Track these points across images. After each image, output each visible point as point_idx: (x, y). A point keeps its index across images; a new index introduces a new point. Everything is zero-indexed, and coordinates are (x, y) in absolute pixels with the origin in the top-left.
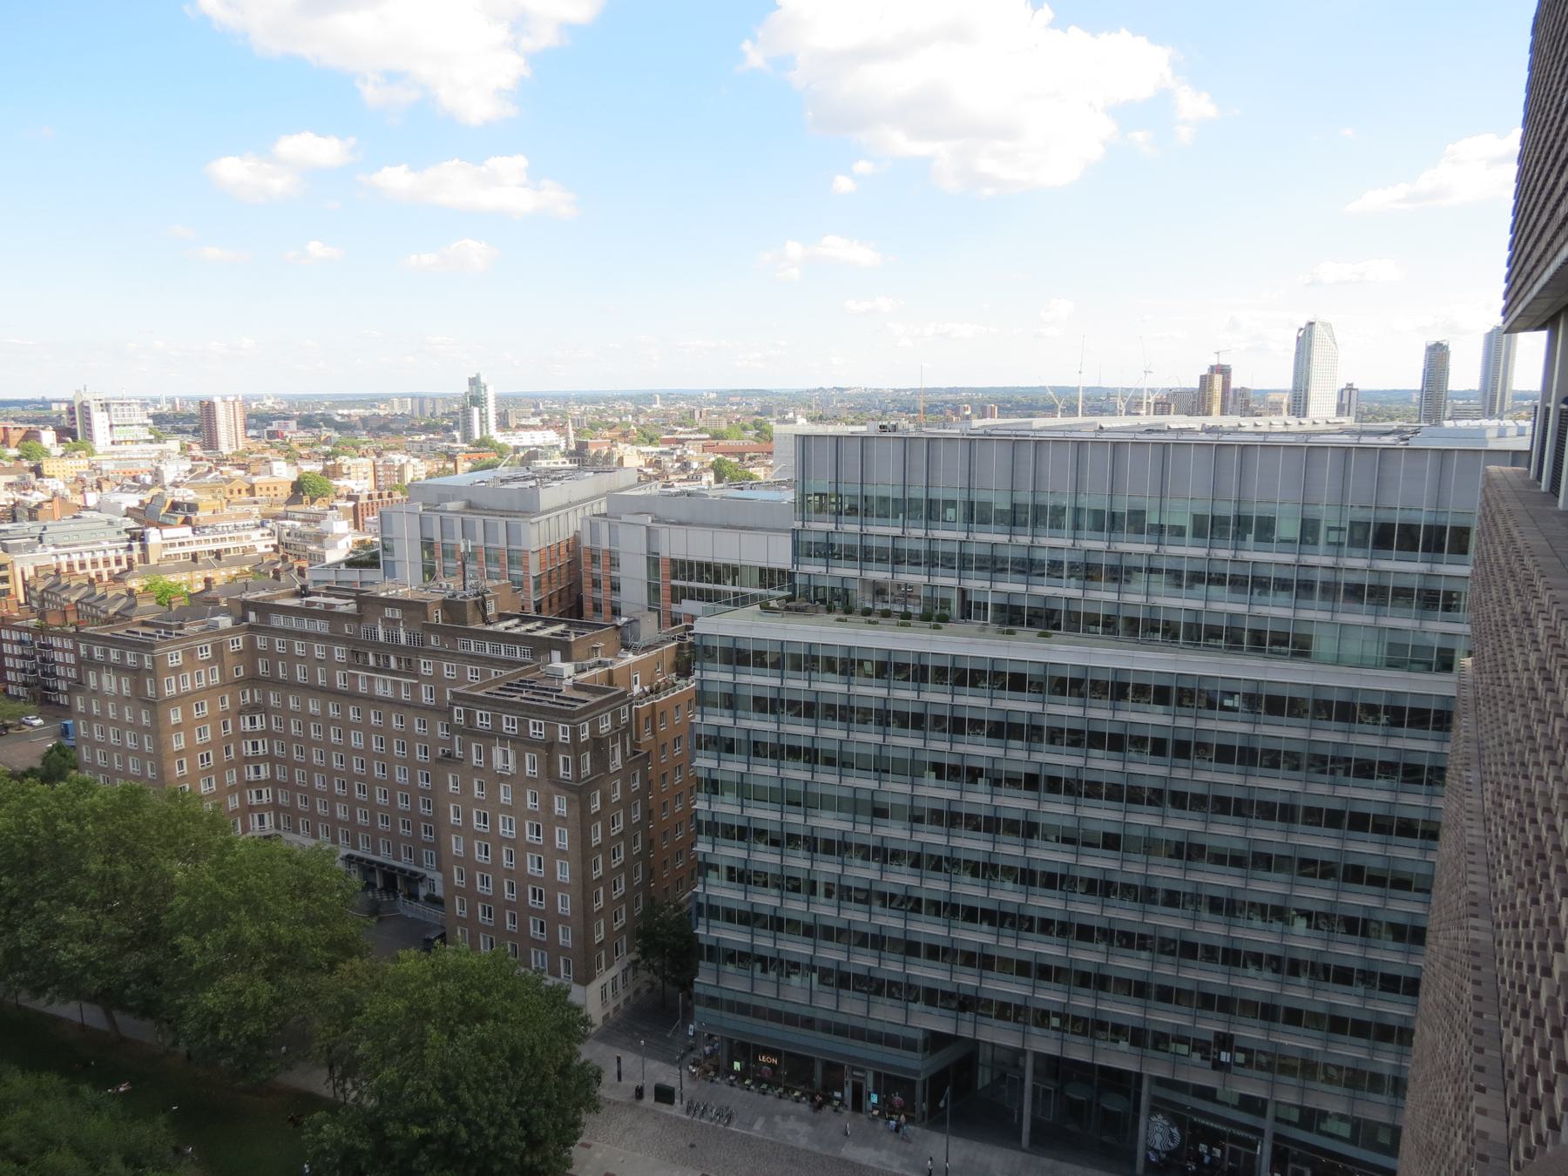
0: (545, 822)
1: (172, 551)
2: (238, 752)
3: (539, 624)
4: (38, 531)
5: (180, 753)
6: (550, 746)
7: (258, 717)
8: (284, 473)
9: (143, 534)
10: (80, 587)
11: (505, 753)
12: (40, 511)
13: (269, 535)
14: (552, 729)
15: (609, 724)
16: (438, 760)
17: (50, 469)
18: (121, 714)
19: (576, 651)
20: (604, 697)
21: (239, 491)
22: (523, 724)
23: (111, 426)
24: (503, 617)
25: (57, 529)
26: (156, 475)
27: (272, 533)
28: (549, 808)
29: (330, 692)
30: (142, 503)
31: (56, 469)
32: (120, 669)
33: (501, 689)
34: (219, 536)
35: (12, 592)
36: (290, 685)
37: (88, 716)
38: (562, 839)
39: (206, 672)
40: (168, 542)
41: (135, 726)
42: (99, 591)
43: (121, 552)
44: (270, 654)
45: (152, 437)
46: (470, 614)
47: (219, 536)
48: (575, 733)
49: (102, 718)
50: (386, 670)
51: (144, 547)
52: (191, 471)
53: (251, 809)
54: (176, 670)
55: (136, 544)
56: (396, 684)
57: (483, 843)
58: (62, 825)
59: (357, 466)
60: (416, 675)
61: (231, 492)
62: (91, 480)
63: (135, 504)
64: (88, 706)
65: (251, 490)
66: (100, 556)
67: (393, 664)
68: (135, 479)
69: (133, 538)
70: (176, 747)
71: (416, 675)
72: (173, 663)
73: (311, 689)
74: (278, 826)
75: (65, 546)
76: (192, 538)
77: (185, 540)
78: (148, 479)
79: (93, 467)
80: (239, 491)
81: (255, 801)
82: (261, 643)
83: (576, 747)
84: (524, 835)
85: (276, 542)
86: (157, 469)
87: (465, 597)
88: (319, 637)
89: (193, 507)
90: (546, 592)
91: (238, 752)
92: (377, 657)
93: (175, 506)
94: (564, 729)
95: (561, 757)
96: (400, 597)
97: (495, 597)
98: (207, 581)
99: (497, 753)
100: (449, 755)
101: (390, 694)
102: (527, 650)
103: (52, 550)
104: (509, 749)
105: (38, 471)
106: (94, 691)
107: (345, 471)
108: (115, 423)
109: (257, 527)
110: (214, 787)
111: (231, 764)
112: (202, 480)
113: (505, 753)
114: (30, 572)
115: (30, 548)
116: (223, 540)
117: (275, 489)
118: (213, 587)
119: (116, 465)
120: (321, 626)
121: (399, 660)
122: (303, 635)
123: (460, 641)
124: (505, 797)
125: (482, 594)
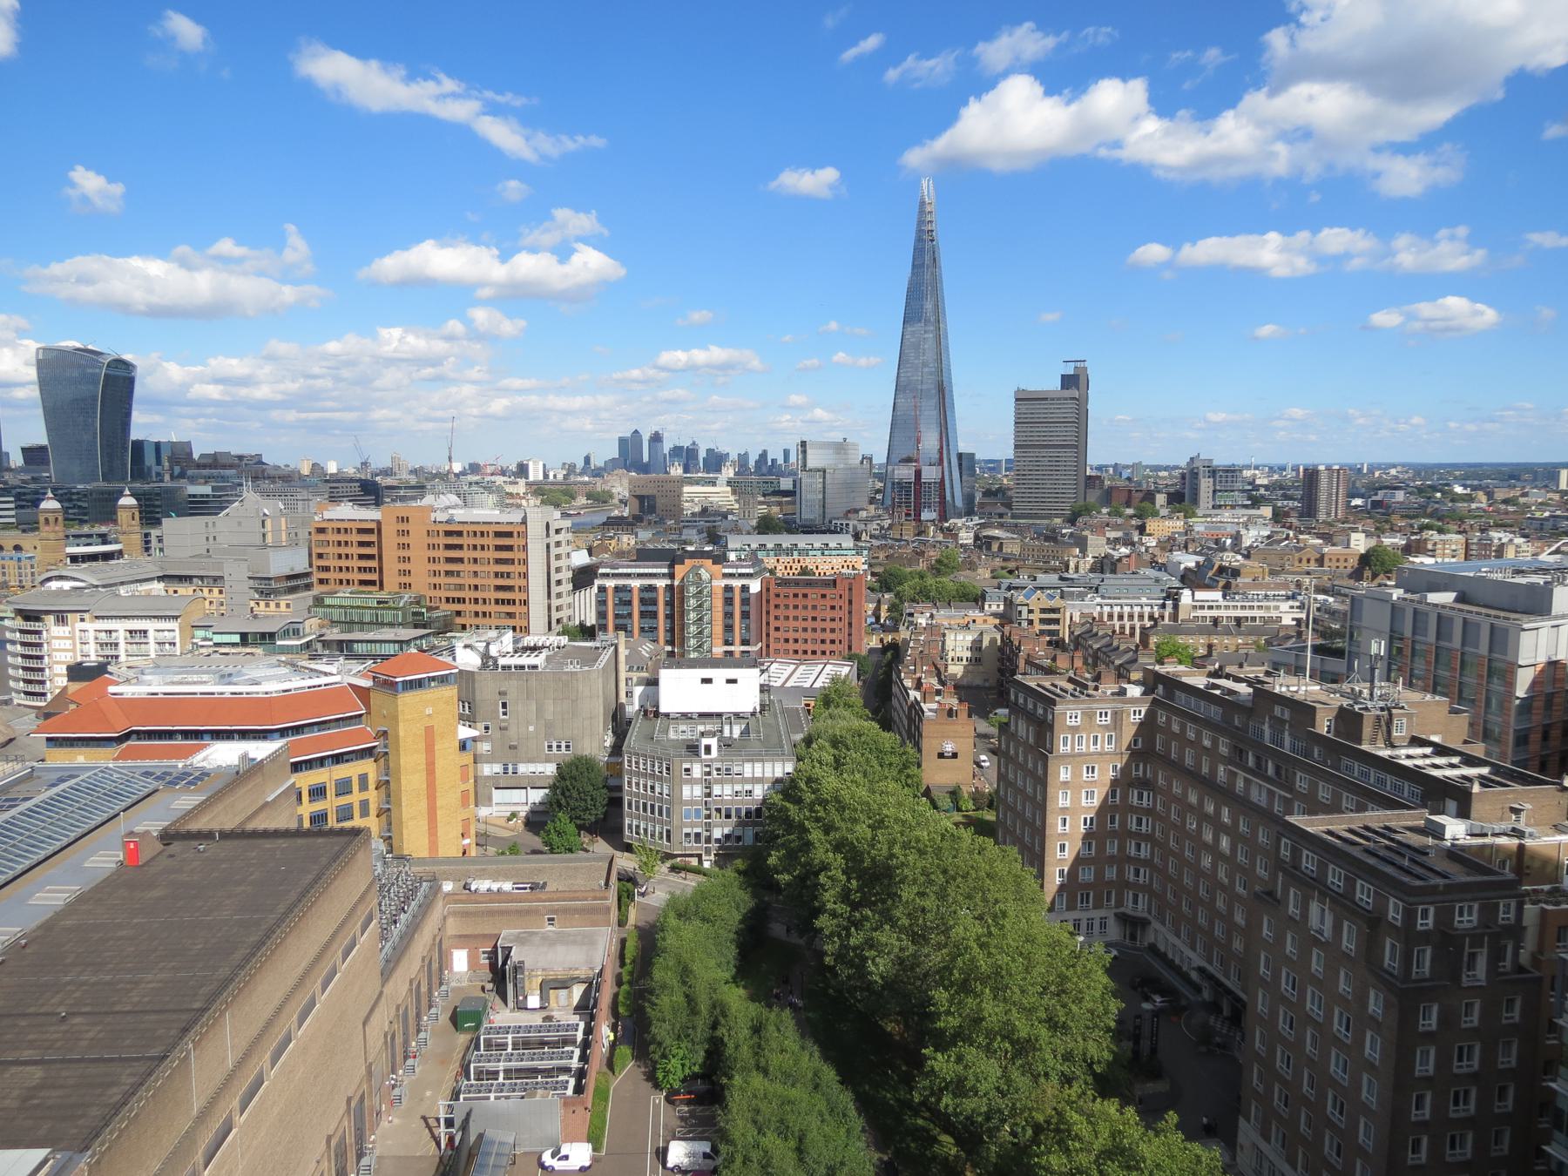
0: (1360, 1021)
2: (1123, 823)
3: (1455, 760)
4: (1097, 582)
5: (1064, 810)
6: (1373, 923)
7: (1145, 794)
8: (1360, 543)
9: (1177, 594)
10: (1107, 635)
11: (1323, 910)
12: (1119, 565)
13: (1298, 607)
14: (1381, 901)
15: (1475, 917)
16: (1256, 895)
18: (1026, 761)
19: (1476, 807)
20: (1486, 878)
21: (1308, 561)
22: (1350, 883)
23: (1214, 491)
24: (1416, 741)
25: (1112, 582)
27: (1301, 607)
28: (1363, 1001)
29: (1208, 785)
30: (1197, 563)
33: (1351, 831)
34: (1247, 604)
36: (1177, 768)
38: (1372, 1048)
39: (1103, 737)
41: (1032, 774)
42: (1115, 643)
43: (1156, 608)
44: (1167, 730)
46: (1367, 730)
47: (1247, 604)
48: (1409, 915)
50: (1259, 771)
51: (1176, 607)
52: (1269, 537)
53: (1128, 885)
54: (1074, 730)
55: (1169, 603)
56: (1271, 793)
57: (1290, 1013)
58: (896, 850)
59: (1444, 542)
60: (1291, 789)
61: (1300, 561)
62: (1181, 539)
63: (1192, 565)
65: (1320, 561)
66: (1137, 609)
67: (1271, 771)
68: (1217, 542)
69: (1167, 597)
70: (1061, 803)
71: (1291, 789)
73: (1194, 777)
74: (1149, 912)
76: (1222, 603)
77: (1214, 604)
78: (1229, 541)
79: (1188, 530)
80: (1308, 561)
81: (1132, 878)
82: (1162, 719)
83: (1409, 936)
84: (1332, 1024)
85: (1303, 616)
86: (1238, 532)
87: (1366, 709)
88: (1207, 723)
89: (1236, 573)
90: (1538, 718)
91: (1123, 823)
92: (1258, 759)
93: (1222, 570)
94: (1508, 906)
95: (1388, 942)
96: (1300, 697)
97: (1410, 716)
98: (1210, 646)
99: (1314, 907)
100: (1271, 894)
101: (1264, 804)
102: (1418, 790)
103: (1099, 600)
104: (1326, 908)
105: (1142, 529)
107: (1430, 547)
109: (1288, 598)
110: (1093, 852)
111: (1113, 834)
112: (1275, 547)
113: (1323, 910)
114: (1077, 619)
115: (1082, 596)
116: (1252, 608)
117: (1346, 560)
118: (1214, 653)
119: (1206, 528)
120: (1215, 712)
121: (1278, 770)
122: (1194, 719)
123: (1346, 761)
124: (1316, 966)
125: (1389, 709)
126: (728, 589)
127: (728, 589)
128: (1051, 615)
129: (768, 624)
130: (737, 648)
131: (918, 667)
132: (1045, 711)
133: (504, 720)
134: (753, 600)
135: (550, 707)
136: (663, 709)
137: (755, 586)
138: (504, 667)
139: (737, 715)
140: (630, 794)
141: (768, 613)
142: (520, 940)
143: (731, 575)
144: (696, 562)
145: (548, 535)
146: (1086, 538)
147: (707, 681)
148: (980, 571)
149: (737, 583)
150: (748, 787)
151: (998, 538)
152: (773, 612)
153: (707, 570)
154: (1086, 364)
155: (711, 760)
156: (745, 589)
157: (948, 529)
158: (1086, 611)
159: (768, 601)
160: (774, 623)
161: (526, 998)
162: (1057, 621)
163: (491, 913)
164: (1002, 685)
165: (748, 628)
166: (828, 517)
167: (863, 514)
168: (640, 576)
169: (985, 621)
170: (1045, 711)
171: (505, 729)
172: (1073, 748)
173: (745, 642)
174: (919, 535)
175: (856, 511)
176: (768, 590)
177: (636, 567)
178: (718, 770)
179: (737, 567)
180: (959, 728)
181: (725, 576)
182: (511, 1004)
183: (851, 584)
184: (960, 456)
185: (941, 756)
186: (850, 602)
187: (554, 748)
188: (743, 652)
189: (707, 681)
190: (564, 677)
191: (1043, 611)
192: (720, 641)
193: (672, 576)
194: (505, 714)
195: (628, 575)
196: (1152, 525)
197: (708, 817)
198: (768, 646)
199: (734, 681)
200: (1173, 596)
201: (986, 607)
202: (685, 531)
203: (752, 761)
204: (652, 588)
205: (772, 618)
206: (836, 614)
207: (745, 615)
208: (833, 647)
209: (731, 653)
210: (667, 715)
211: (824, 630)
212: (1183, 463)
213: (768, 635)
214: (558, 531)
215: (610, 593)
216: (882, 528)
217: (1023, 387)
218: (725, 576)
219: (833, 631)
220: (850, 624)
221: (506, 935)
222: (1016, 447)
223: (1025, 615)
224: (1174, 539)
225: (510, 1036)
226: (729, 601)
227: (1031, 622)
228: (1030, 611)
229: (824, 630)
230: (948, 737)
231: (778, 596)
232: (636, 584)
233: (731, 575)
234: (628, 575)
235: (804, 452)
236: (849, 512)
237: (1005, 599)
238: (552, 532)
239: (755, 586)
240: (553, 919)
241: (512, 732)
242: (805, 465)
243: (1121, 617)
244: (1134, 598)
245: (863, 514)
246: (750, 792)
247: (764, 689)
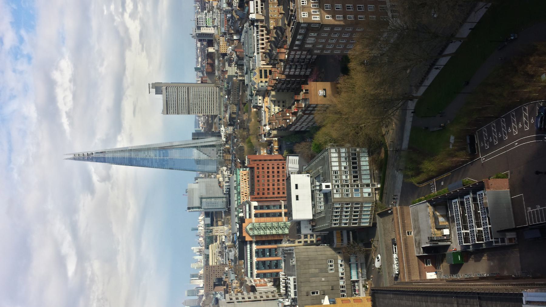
1: (260, 10)
9: (251, 21)
17: (223, 50)
18: (324, 38)
23: (207, 27)
26: (227, 12)
31: (223, 49)
32: (305, 36)
35: (270, 69)
37: (322, 49)
40: (255, 11)
41: (330, 33)
42: (273, 39)
45: (211, 12)
49: (324, 45)
51: (257, 21)
64: (318, 49)
72: (306, 16)
75: (254, 49)
103: (255, 54)
105: (224, 55)
106: (313, 46)
108: (205, 25)
114: (263, 62)
115: (254, 61)
126: (256, 216)
127: (256, 216)
128: (264, 74)
129: (271, 198)
130: (283, 211)
131: (287, 118)
132: (302, 28)
133: (320, 293)
134: (261, 204)
135: (313, 271)
136: (311, 217)
137: (255, 204)
138: (295, 295)
139: (312, 183)
140: (350, 223)
141: (266, 198)
142: (419, 244)
143: (250, 214)
144: (244, 231)
145: (233, 302)
146: (229, 76)
147: (297, 197)
148: (245, 119)
149: (253, 212)
150: (343, 168)
151: (230, 115)
152: (266, 195)
153: (247, 226)
154: (151, 83)
155: (332, 185)
156: (256, 208)
157: (226, 139)
158: (260, 59)
159: (261, 198)
160: (271, 195)
161: (445, 235)
162: (266, 71)
163: (408, 261)
164: (294, 89)
165: (274, 206)
166: (222, 195)
167: (221, 179)
168: (251, 257)
169: (267, 102)
170: (302, 28)
171: (324, 292)
172: (318, 15)
173: (280, 208)
174: (229, 152)
175: (220, 183)
176: (256, 198)
177: (247, 260)
178: (336, 181)
179: (246, 212)
180: (313, 88)
181: (250, 217)
182: (449, 243)
183: (252, 161)
184: (193, 139)
185: (325, 96)
186: (260, 160)
187: (332, 268)
188: (284, 208)
189: (297, 197)
190: (299, 264)
191: (261, 77)
192: (280, 218)
193: (251, 243)
194: (317, 293)
195: (251, 263)
196: (222, 51)
197: (358, 186)
198: (281, 197)
199: (297, 186)
200: (253, 21)
201: (260, 105)
202: (230, 258)
203: (331, 166)
204: (258, 263)
205: (269, 196)
206: (266, 166)
207: (268, 207)
208: (281, 167)
209: (285, 214)
210: (314, 216)
211: (273, 172)
212: (194, 40)
213: (277, 198)
214: (231, 299)
215: (260, 271)
216: (227, 170)
217: (161, 112)
218: (250, 217)
219: (273, 168)
220: (270, 160)
221: (416, 252)
222: (189, 113)
223: (263, 84)
224: (228, 39)
225: (462, 231)
226: (262, 215)
227: (266, 82)
228: (261, 82)
229: (273, 172)
230: (317, 93)
231: (258, 194)
232: (255, 259)
233: (250, 214)
234: (251, 263)
235: (193, 208)
236: (220, 186)
237: (256, 95)
238: (231, 301)
239: (255, 204)
240: (408, 233)
241: (324, 288)
242: (199, 208)
243: (263, 40)
244: (254, 39)
245: (221, 179)
246: (345, 168)
247: (300, 172)
